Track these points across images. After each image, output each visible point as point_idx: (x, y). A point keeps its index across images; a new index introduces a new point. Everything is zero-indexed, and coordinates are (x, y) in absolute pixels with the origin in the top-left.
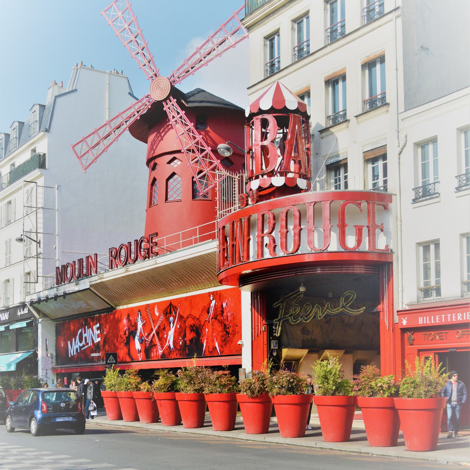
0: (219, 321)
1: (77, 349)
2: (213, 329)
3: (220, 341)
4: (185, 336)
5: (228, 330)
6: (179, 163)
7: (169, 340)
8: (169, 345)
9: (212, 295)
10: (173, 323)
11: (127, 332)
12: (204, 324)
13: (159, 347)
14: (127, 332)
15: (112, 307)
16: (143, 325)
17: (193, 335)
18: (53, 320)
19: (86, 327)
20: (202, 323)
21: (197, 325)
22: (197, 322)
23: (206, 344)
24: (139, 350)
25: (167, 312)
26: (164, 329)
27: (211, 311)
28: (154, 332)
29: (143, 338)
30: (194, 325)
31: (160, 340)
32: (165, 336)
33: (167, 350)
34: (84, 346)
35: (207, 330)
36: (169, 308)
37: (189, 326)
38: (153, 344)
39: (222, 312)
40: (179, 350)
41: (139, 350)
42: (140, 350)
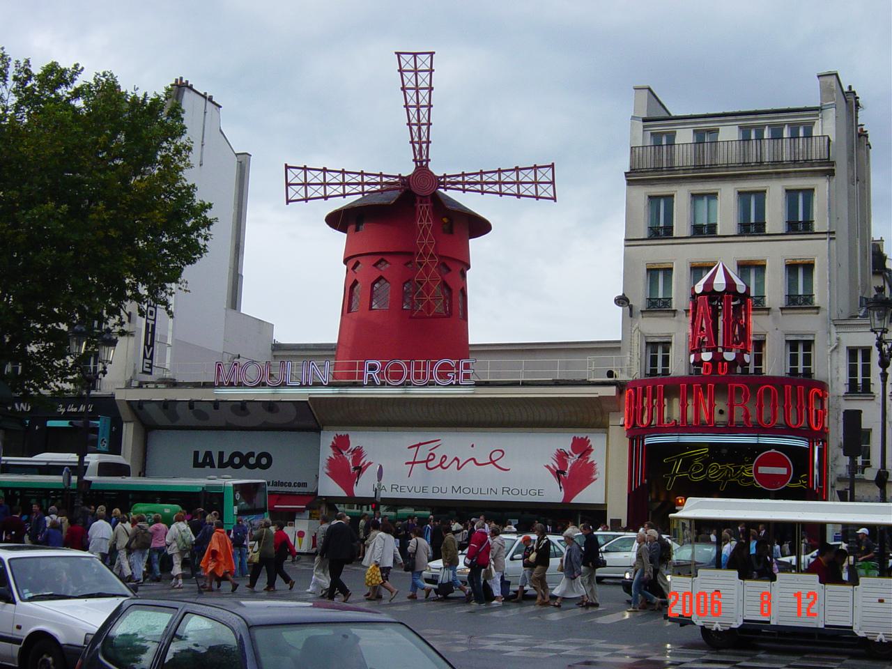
15: (319, 427)
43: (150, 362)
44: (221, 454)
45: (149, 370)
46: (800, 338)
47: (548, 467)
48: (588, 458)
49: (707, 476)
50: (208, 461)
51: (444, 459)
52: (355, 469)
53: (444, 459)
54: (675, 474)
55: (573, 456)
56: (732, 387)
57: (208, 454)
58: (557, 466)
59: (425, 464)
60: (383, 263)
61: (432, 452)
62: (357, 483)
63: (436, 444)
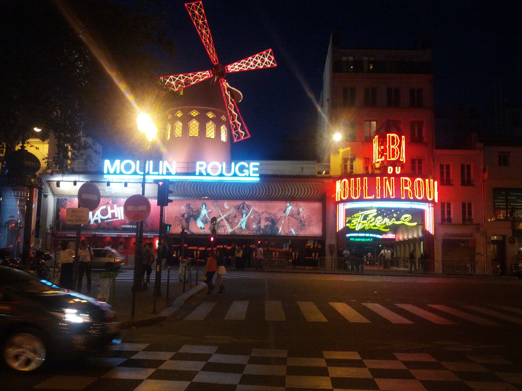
0: (296, 218)
1: (96, 221)
2: (289, 221)
3: (296, 229)
4: (259, 222)
5: (304, 223)
7: (241, 225)
8: (241, 227)
9: (289, 203)
10: (246, 215)
11: (186, 216)
12: (280, 218)
13: (228, 226)
14: (186, 216)
16: (209, 213)
17: (267, 223)
19: (115, 206)
20: (278, 218)
21: (273, 219)
22: (273, 217)
23: (283, 229)
24: (202, 227)
25: (239, 207)
26: (235, 217)
27: (288, 212)
28: (223, 217)
29: (208, 220)
30: (269, 218)
31: (228, 222)
32: (236, 221)
33: (238, 229)
34: (108, 219)
35: (283, 222)
36: (242, 205)
37: (264, 218)
38: (220, 225)
39: (299, 213)
40: (252, 230)
41: (202, 227)
42: (203, 228)
49: (376, 223)
60: (194, 112)
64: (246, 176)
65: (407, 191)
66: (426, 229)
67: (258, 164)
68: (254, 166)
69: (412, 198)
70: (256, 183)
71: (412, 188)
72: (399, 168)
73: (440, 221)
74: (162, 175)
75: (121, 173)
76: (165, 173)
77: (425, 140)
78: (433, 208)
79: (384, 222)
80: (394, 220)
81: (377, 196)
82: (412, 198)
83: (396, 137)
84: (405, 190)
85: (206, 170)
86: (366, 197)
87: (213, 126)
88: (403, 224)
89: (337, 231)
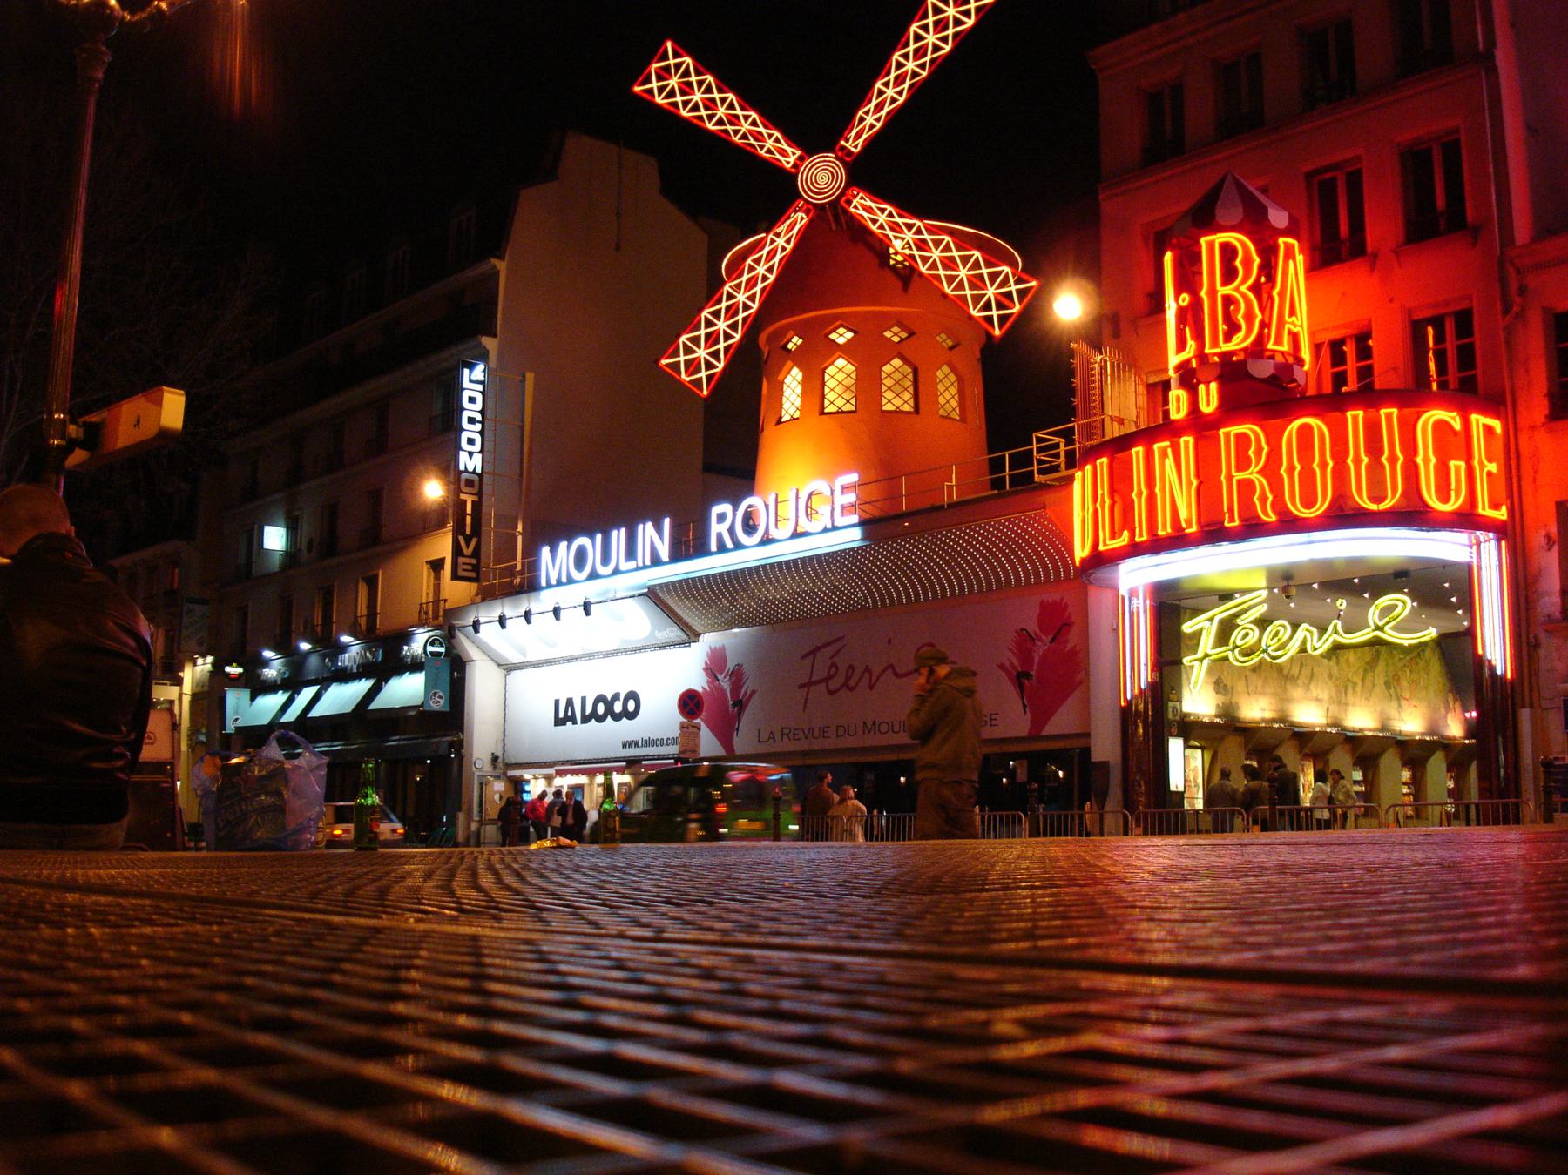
6: (850, 335)
18: (499, 665)
43: (474, 561)
44: (584, 700)
45: (473, 575)
46: (1443, 311)
47: (1002, 667)
48: (1066, 642)
50: (569, 714)
51: (850, 672)
52: (734, 705)
53: (850, 672)
54: (1207, 656)
55: (1041, 640)
56: (1227, 435)
57: (570, 702)
58: (1016, 662)
59: (824, 685)
61: (836, 660)
62: (738, 729)
63: (840, 644)
64: (825, 530)
65: (1247, 486)
66: (1480, 652)
67: (853, 478)
68: (844, 489)
69: (1273, 518)
70: (852, 549)
71: (1270, 471)
72: (1213, 386)
73: (1550, 602)
74: (645, 567)
75: (571, 581)
76: (648, 562)
77: (1471, 214)
78: (1503, 543)
79: (1293, 648)
80: (1335, 626)
81: (1137, 530)
82: (1273, 518)
83: (1239, 240)
84: (1239, 482)
85: (731, 531)
86: (1105, 544)
87: (850, 368)
88: (1376, 643)
89: (1123, 704)
